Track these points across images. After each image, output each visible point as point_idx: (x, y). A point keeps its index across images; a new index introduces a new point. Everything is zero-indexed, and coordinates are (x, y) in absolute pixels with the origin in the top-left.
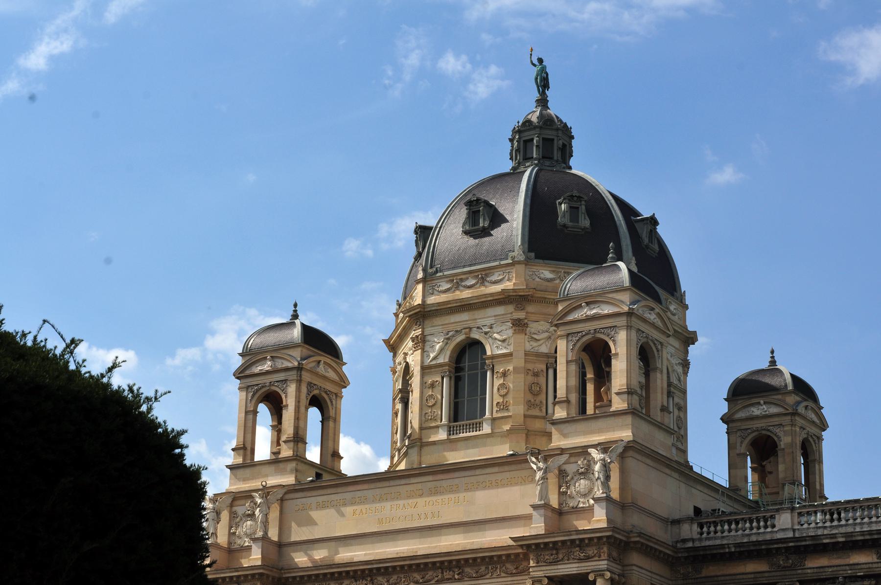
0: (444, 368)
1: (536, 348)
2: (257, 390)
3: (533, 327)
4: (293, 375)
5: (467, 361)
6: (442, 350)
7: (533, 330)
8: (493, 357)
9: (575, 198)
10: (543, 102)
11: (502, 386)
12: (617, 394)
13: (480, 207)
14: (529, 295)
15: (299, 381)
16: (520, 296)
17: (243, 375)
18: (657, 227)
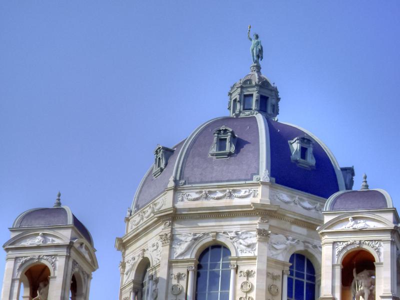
0: (190, 263)
1: (275, 256)
2: (26, 261)
3: (274, 238)
4: (64, 252)
5: (209, 260)
6: (189, 248)
7: (273, 241)
8: (238, 259)
9: (306, 141)
10: (258, 68)
11: (245, 283)
12: (382, 297)
13: (227, 136)
14: (273, 211)
15: (68, 257)
16: (266, 210)
17: (13, 247)
18: (354, 177)
